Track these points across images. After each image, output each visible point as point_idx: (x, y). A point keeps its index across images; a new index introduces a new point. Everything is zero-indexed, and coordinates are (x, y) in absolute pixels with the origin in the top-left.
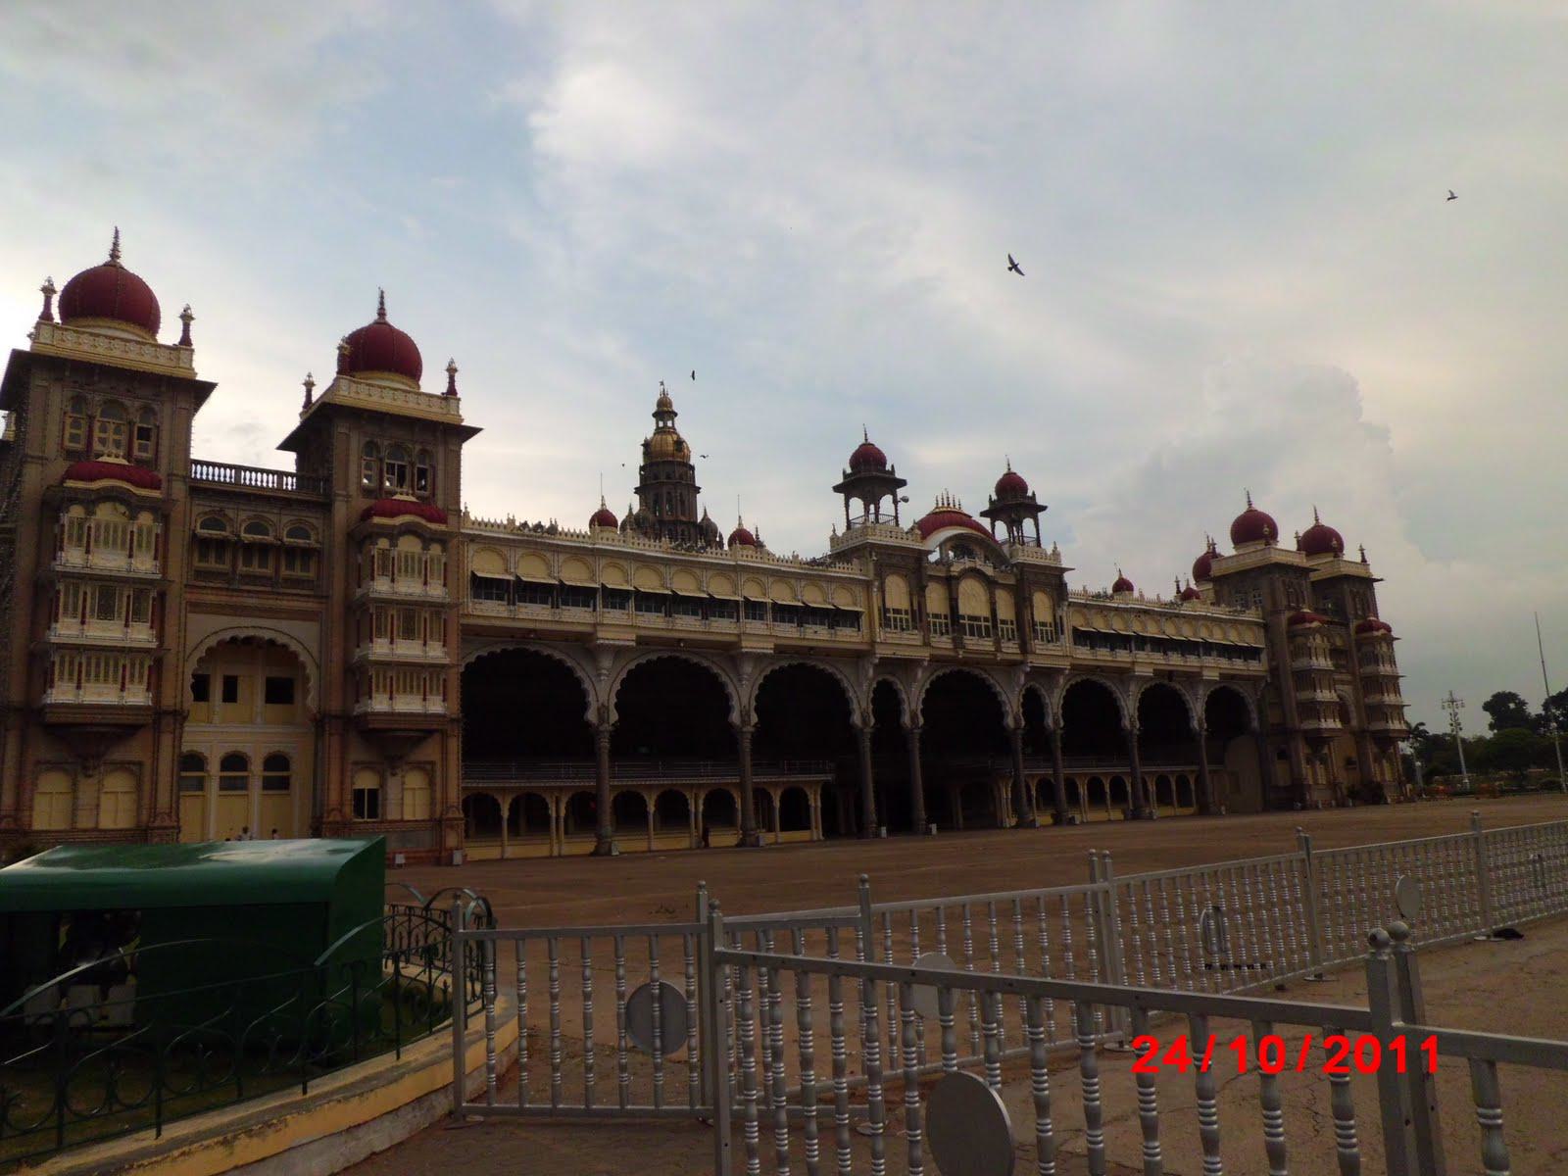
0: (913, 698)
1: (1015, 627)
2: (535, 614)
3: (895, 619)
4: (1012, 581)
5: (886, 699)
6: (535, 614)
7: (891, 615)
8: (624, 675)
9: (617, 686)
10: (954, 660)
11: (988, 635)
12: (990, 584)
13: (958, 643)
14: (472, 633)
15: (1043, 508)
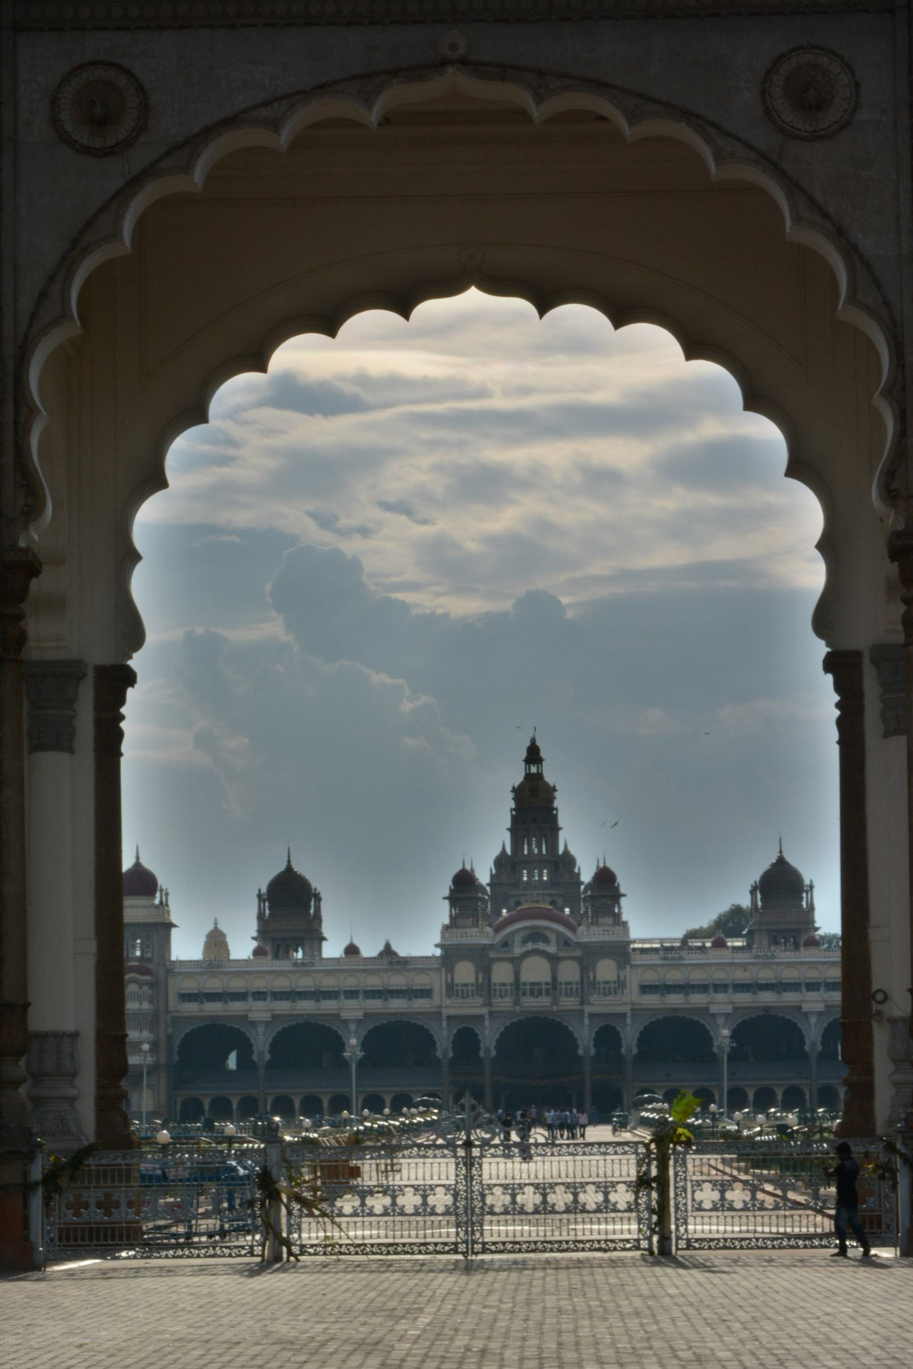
0: (489, 1037)
1: (579, 986)
2: (213, 1008)
3: (462, 991)
4: (578, 953)
5: (466, 1039)
6: (213, 1008)
7: (460, 988)
8: (274, 1034)
9: (270, 1041)
10: (514, 1012)
11: (548, 993)
12: (554, 960)
13: (517, 1002)
14: (177, 1020)
15: (624, 895)
